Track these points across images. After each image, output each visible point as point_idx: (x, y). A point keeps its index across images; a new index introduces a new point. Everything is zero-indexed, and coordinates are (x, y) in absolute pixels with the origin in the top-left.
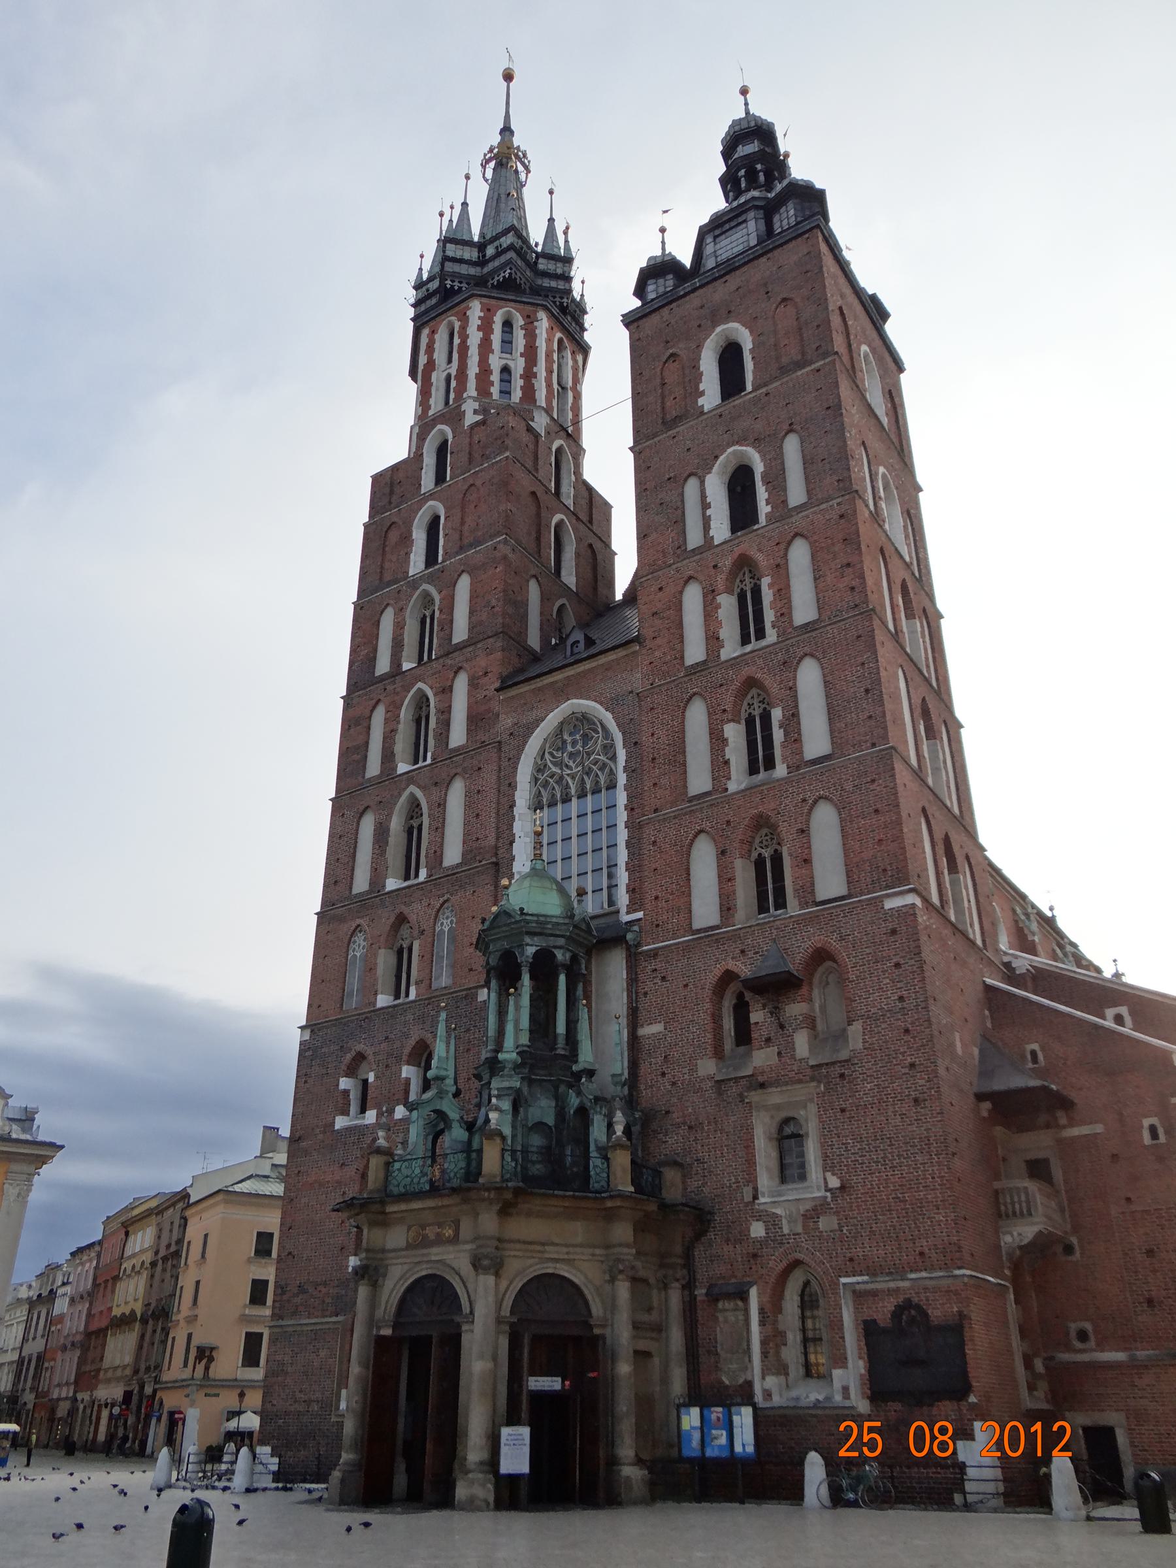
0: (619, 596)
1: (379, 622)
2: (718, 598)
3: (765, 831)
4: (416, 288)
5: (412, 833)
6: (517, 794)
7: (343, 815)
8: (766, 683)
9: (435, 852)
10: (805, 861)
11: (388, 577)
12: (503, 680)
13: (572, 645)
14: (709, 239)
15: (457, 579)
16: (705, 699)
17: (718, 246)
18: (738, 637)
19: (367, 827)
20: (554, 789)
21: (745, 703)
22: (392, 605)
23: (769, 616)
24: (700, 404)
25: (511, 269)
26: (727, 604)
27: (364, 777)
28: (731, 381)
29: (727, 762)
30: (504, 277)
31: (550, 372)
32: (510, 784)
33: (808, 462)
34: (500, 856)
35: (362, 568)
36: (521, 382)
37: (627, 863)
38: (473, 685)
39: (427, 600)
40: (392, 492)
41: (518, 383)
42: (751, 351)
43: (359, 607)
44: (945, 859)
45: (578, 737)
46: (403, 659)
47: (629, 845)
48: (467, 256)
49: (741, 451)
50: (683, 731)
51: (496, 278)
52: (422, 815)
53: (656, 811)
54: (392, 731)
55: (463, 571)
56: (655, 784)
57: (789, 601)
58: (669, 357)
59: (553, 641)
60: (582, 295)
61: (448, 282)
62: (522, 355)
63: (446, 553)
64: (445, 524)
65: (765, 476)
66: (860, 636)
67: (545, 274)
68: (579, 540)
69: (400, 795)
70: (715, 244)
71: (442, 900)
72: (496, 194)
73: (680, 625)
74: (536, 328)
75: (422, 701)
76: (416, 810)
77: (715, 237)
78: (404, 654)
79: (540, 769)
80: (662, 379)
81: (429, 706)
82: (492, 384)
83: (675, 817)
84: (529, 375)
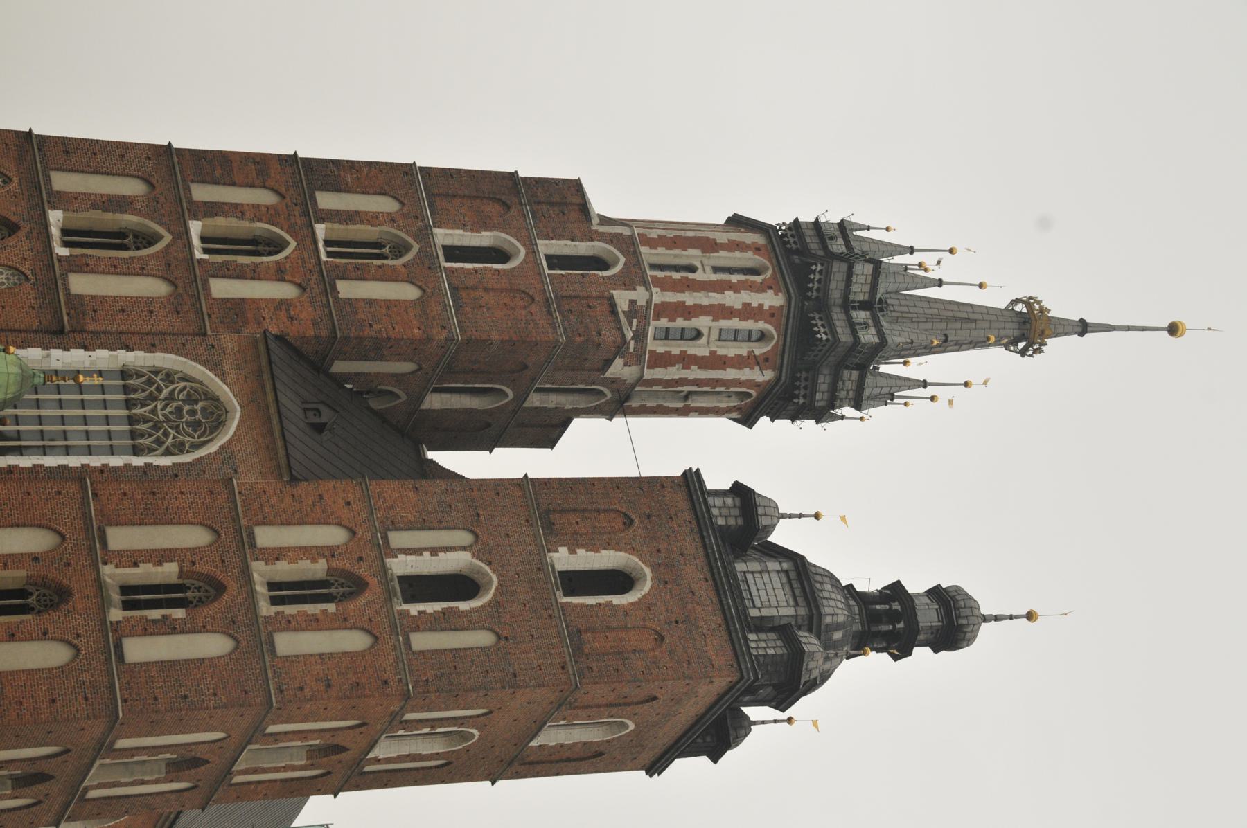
0: (431, 455)
1: (385, 194)
2: (324, 561)
3: (56, 599)
4: (843, 226)
5: (118, 239)
6: (140, 354)
7: (149, 158)
8: (216, 604)
9: (87, 265)
10: (13, 635)
11: (439, 202)
12: (281, 338)
13: (318, 410)
14: (785, 566)
15: (416, 285)
16: (211, 545)
17: (774, 575)
18: (278, 579)
19: (131, 187)
20: (144, 391)
21: (198, 584)
22: (401, 210)
23: (290, 610)
24: (560, 549)
25: (827, 340)
26: (318, 569)
27: (193, 181)
28: (577, 582)
29: (136, 565)
30: (818, 332)
31: (697, 382)
32: (153, 345)
33: (456, 653)
34: (71, 335)
35: (459, 171)
36: (676, 351)
37: (42, 466)
38: (281, 305)
39: (400, 249)
40: (553, 204)
41: (675, 348)
42: (609, 604)
43: (407, 170)
44: (19, 772)
45: (199, 416)
46: (330, 225)
47: (65, 467)
48: (855, 288)
49: (488, 590)
50: (179, 523)
51: (820, 323)
52: (138, 248)
53: (95, 495)
54: (243, 213)
55: (424, 291)
56: (125, 494)
57: (302, 630)
58: (629, 517)
59: (348, 386)
60: (843, 417)
61: (819, 268)
62: (713, 353)
63: (452, 271)
64: (491, 269)
65: (454, 611)
66: (246, 692)
67: (836, 379)
68: (490, 413)
69: (161, 224)
70: (778, 572)
71: (28, 273)
72: (980, 317)
73: (302, 522)
74: (752, 368)
75: (276, 245)
76: (144, 242)
77: (787, 572)
78: (336, 226)
79: (169, 377)
80: (606, 511)
81: (270, 254)
82: (672, 319)
83: (84, 513)
84: (686, 360)
